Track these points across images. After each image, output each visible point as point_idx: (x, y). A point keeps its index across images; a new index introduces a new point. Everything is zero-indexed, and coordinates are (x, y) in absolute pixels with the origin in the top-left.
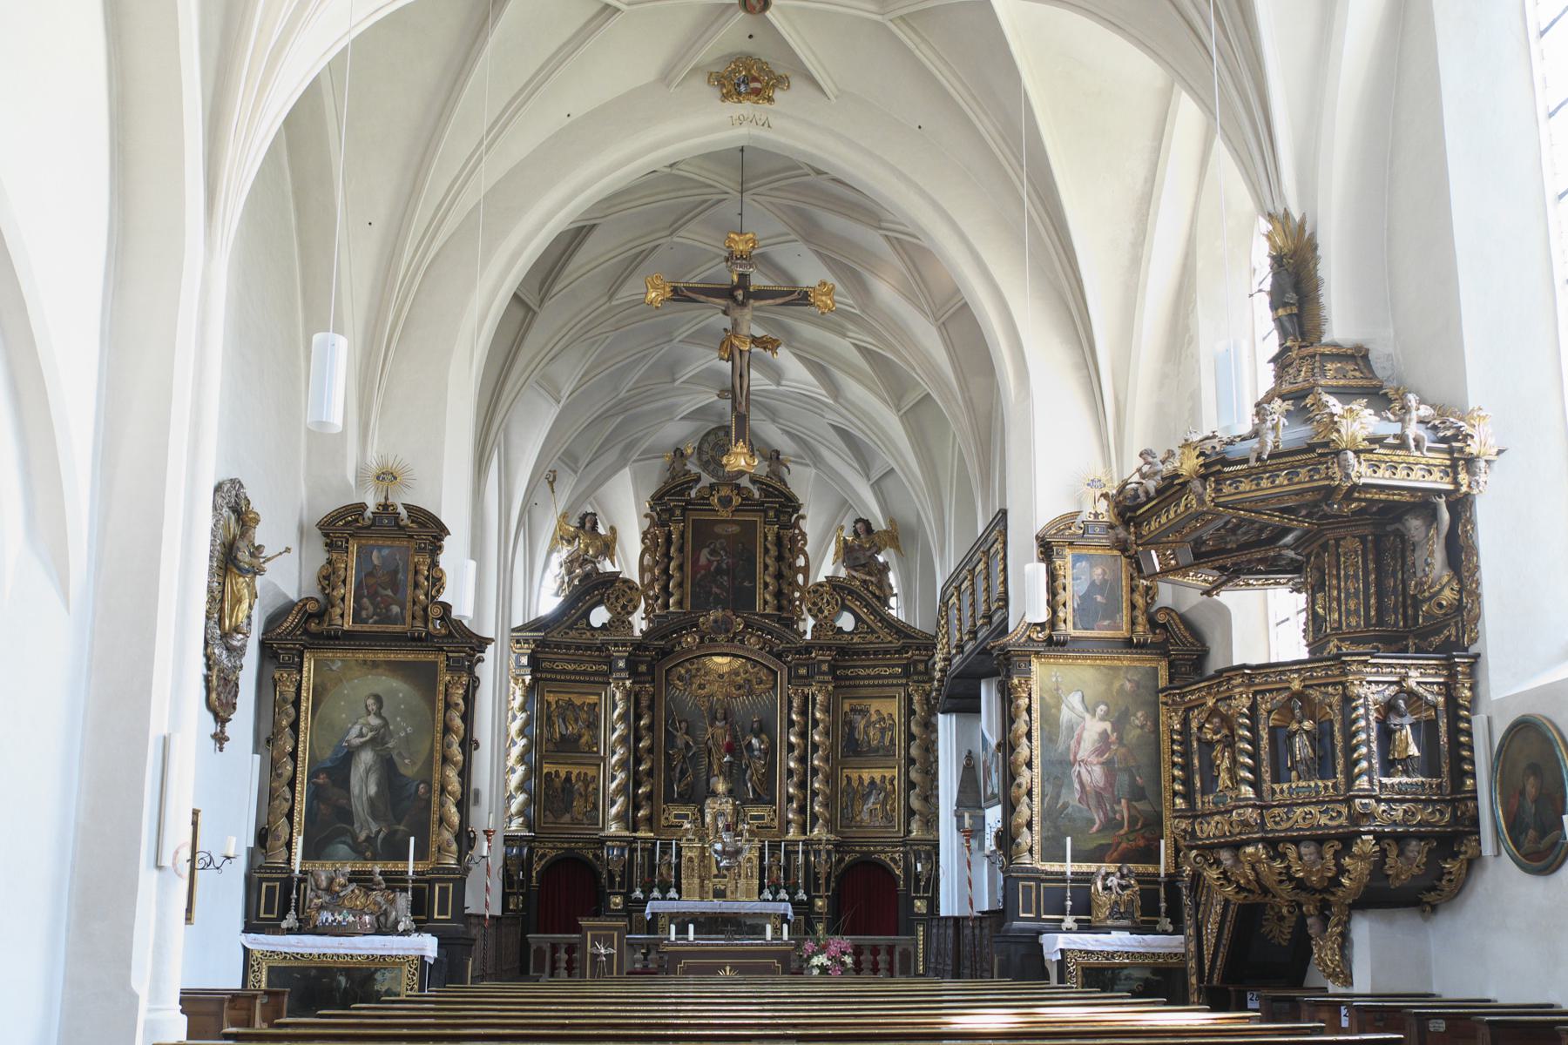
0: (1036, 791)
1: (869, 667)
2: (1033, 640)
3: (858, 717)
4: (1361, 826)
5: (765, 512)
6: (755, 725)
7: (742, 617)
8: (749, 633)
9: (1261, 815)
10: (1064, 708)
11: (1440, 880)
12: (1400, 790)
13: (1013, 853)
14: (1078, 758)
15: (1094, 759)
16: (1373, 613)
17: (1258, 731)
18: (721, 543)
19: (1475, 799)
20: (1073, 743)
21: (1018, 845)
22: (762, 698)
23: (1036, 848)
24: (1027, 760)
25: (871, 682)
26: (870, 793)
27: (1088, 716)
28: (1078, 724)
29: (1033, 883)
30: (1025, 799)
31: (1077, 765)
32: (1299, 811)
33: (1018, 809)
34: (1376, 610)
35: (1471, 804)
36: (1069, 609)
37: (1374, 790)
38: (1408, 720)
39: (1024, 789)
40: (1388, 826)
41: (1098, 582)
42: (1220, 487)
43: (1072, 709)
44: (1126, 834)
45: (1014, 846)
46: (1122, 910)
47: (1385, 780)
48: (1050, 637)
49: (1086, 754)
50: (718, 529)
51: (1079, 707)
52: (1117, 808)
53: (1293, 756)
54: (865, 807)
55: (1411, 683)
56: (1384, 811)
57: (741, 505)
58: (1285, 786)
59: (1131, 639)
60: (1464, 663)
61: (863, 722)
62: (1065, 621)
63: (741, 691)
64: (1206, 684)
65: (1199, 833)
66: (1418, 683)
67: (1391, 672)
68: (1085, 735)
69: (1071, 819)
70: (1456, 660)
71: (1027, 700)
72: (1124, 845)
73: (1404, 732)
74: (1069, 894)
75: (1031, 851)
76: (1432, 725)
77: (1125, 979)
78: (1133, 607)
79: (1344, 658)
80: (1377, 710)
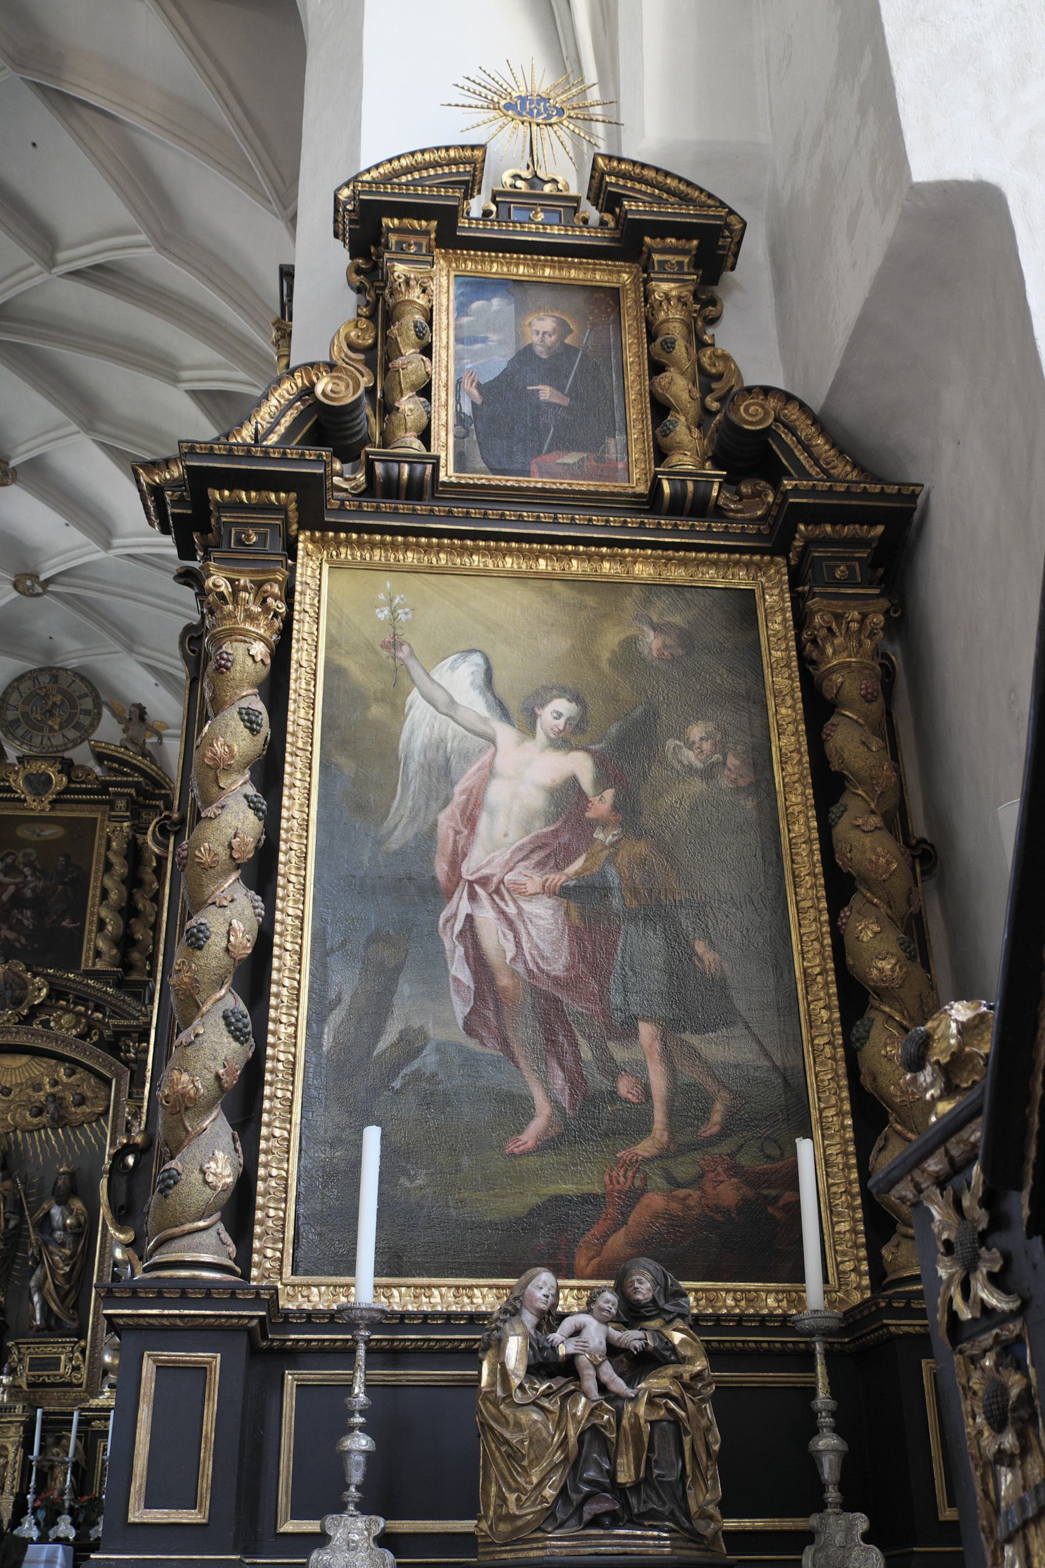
5: (111, 804)
6: (60, 1183)
7: (46, 976)
8: (62, 1008)
18: (25, 855)
22: (84, 1134)
50: (23, 832)
57: (67, 791)
63: (44, 1119)
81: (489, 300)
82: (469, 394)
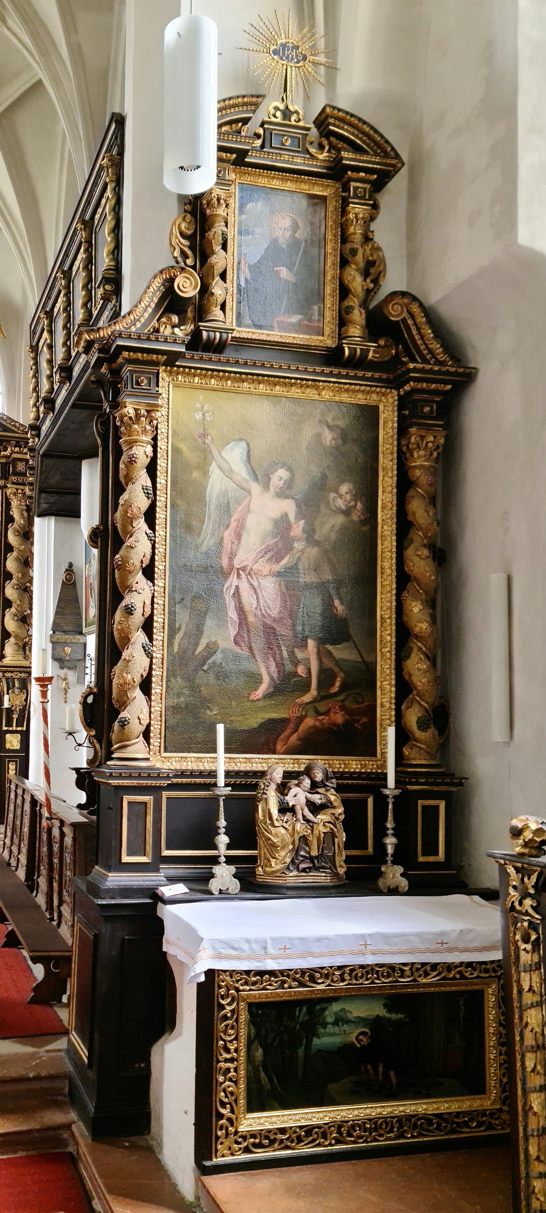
10: (214, 471)
13: (114, 737)
14: (237, 563)
15: (263, 566)
20: (228, 535)
21: (124, 724)
23: (156, 728)
24: (146, 562)
27: (256, 488)
28: (238, 502)
29: (148, 798)
30: (139, 637)
31: (234, 575)
33: (125, 654)
39: (138, 618)
41: (283, 242)
43: (228, 473)
44: (315, 701)
48: (196, 334)
49: (252, 555)
51: (241, 470)
52: (300, 654)
59: (340, 349)
62: (223, 307)
68: (251, 522)
69: (221, 675)
72: (309, 722)
74: (222, 823)
75: (146, 734)
77: (336, 1023)
78: (344, 291)
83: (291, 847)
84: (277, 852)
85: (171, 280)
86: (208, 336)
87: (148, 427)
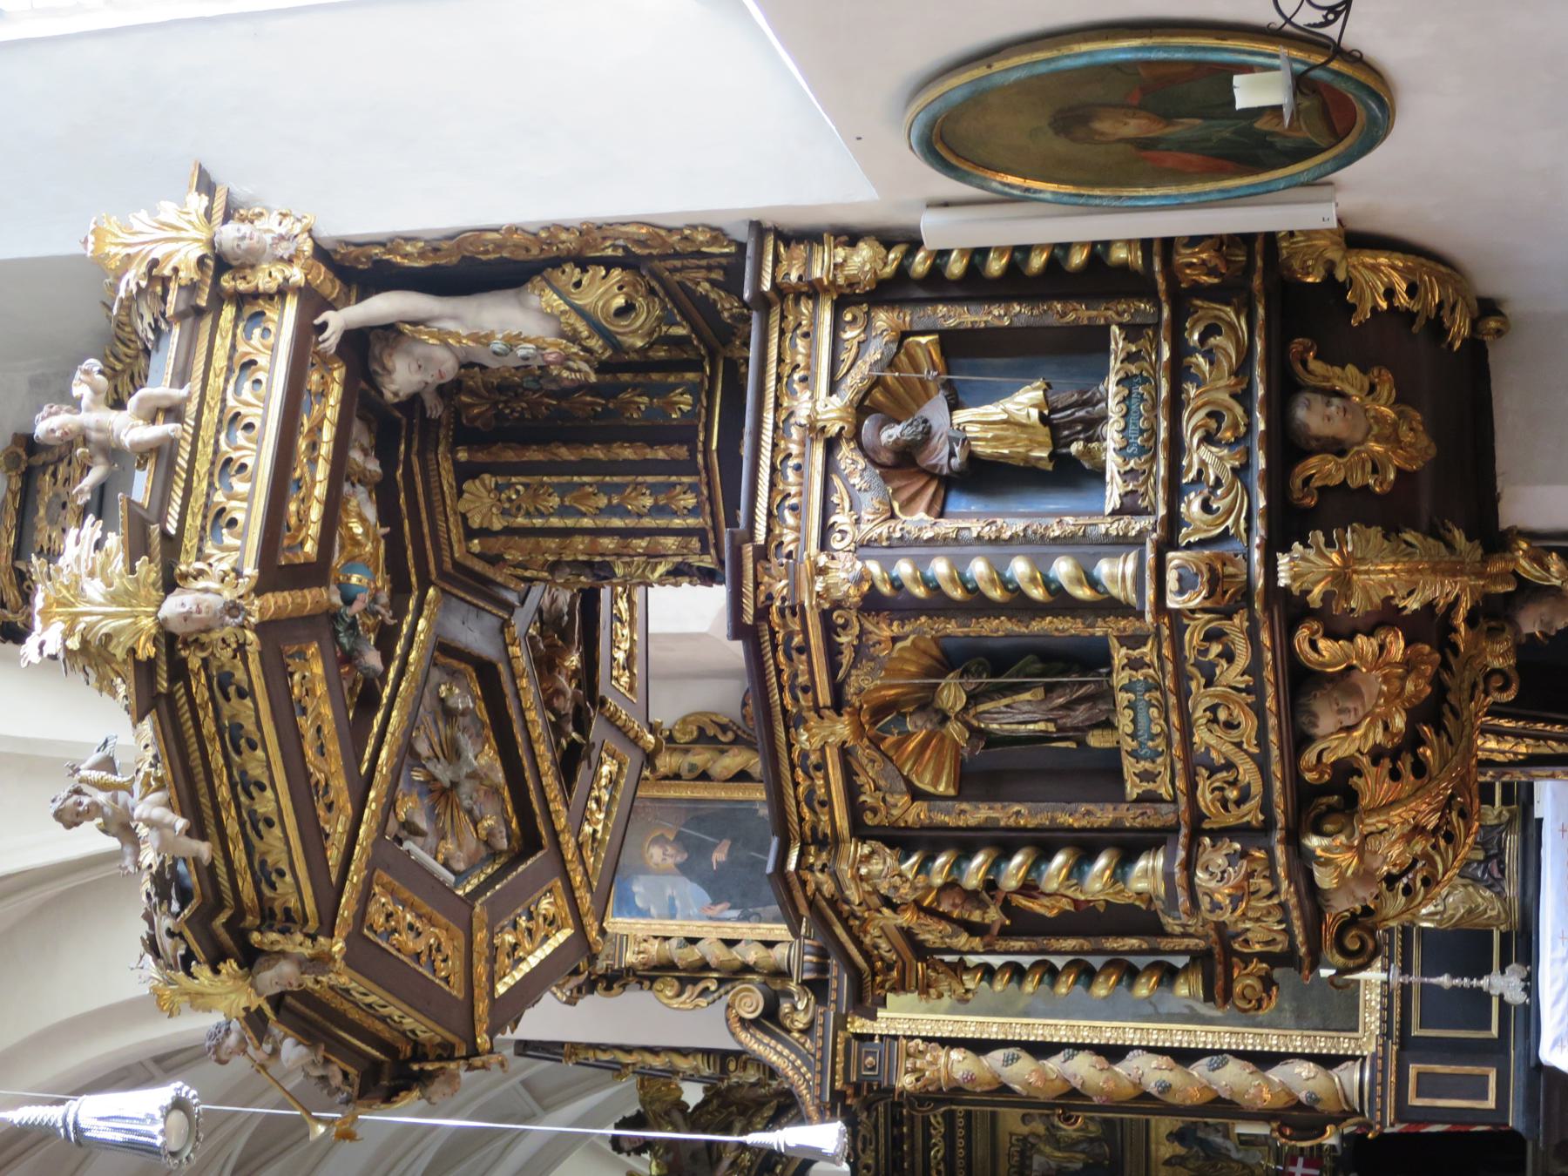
0: (1180, 1036)
1: (927, 1137)
2: (812, 1023)
3: (1037, 1161)
4: (1249, 583)
9: (1218, 834)
11: (1409, 316)
12: (1142, 450)
16: (661, 454)
17: (969, 829)
19: (1168, 243)
24: (1101, 1061)
25: (961, 1132)
26: (1203, 1143)
30: (1200, 1069)
32: (1201, 736)
34: (651, 444)
35: (1184, 256)
36: (742, 930)
37: (1142, 533)
38: (936, 411)
40: (1248, 490)
41: (682, 857)
42: (280, 915)
45: (1319, 1107)
46: (1480, 856)
47: (1113, 495)
53: (1044, 738)
54: (1234, 1155)
55: (831, 410)
56: (1206, 507)
58: (1130, 767)
60: (777, 260)
61: (1048, 1149)
64: (839, 930)
65: (1278, 949)
66: (833, 388)
67: (798, 468)
70: (766, 286)
71: (956, 1055)
73: (973, 430)
75: (1328, 1061)
76: (954, 344)
79: (748, 619)
80: (907, 505)
81: (633, 894)
82: (722, 911)
83: (1471, 889)
84: (1478, 906)
85: (742, 1020)
86: (810, 970)
87: (928, 1057)
